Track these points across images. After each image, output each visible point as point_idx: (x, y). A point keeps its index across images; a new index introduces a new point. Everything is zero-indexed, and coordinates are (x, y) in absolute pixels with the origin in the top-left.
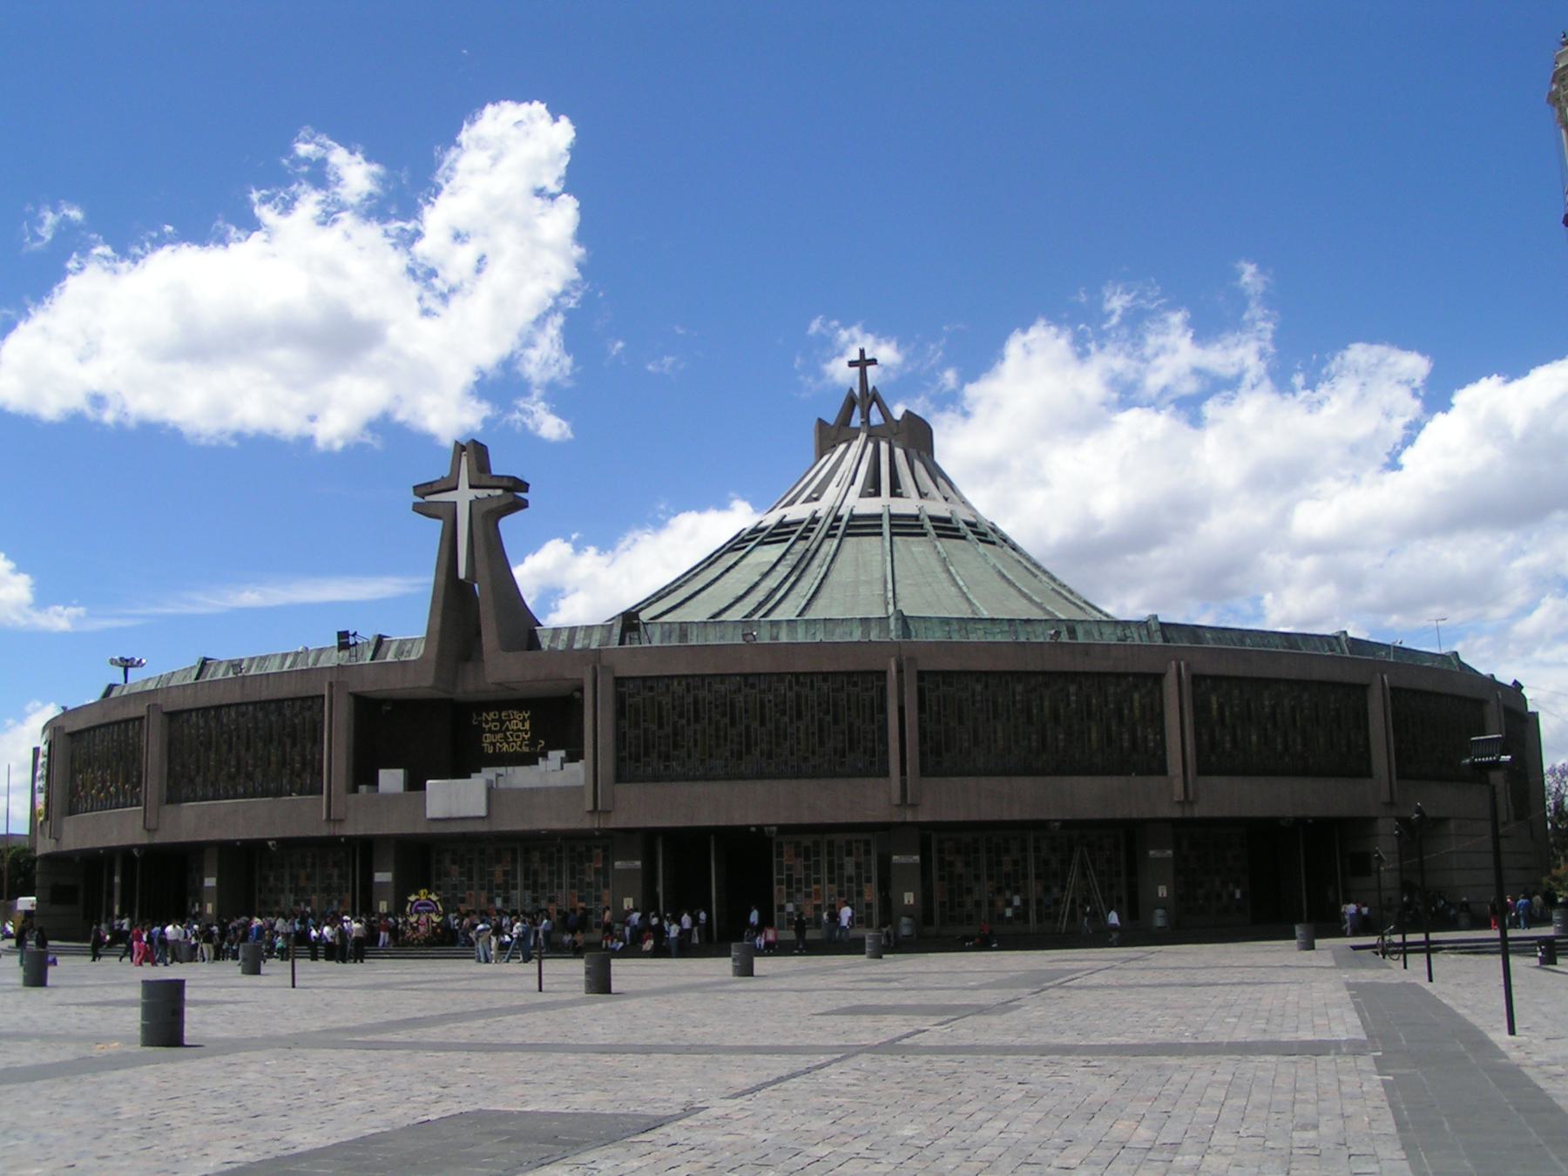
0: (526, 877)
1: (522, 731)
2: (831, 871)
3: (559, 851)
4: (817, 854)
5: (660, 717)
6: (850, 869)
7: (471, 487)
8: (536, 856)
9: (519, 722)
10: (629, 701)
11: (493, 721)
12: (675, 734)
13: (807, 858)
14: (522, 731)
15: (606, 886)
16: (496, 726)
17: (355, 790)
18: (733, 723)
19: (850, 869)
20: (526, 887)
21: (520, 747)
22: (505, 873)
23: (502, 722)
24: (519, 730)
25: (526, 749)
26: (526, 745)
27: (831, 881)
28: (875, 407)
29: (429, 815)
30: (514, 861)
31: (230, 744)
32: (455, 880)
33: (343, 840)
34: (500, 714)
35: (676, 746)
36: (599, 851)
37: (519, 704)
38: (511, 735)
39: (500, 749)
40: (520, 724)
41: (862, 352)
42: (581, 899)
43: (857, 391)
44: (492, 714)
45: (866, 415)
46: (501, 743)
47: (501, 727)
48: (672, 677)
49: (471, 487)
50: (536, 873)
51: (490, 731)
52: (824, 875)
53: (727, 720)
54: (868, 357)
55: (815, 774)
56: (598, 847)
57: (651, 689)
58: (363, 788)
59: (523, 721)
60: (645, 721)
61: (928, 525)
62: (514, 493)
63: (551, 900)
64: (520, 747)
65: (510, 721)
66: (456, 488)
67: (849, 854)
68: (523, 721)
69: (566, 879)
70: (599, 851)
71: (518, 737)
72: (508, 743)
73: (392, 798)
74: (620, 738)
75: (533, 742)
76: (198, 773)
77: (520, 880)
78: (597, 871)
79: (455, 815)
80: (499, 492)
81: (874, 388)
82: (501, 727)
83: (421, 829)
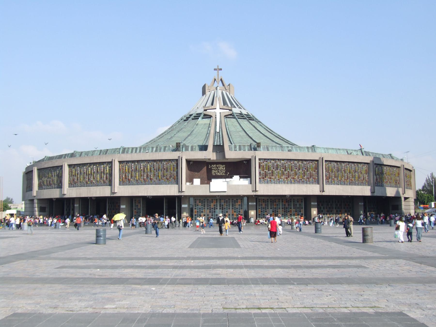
0: (220, 206)
1: (223, 170)
2: (294, 206)
3: (229, 200)
4: (291, 202)
5: (269, 169)
6: (298, 206)
8: (223, 201)
9: (222, 168)
10: (261, 164)
11: (215, 167)
12: (272, 173)
13: (289, 203)
14: (223, 170)
15: (242, 209)
16: (216, 169)
17: (186, 184)
18: (285, 170)
19: (298, 206)
20: (220, 209)
21: (223, 174)
22: (214, 205)
23: (217, 168)
24: (222, 170)
25: (224, 175)
26: (224, 174)
27: (294, 208)
30: (217, 202)
31: (144, 172)
32: (199, 207)
33: (183, 196)
34: (217, 165)
35: (272, 176)
36: (240, 200)
37: (222, 163)
38: (220, 171)
39: (217, 174)
40: (222, 169)
42: (235, 212)
44: (214, 165)
46: (217, 173)
47: (217, 169)
48: (271, 159)
49: (220, 109)
50: (223, 205)
51: (214, 170)
52: (292, 207)
53: (284, 170)
54: (219, 68)
55: (303, 182)
56: (239, 199)
57: (267, 162)
59: (223, 167)
60: (265, 169)
61: (235, 115)
63: (227, 212)
64: (223, 174)
65: (220, 167)
66: (216, 109)
67: (298, 202)
68: (223, 167)
69: (231, 207)
70: (240, 200)
71: (222, 171)
72: (219, 173)
73: (197, 186)
74: (260, 172)
75: (226, 173)
76: (132, 177)
77: (218, 207)
78: (239, 205)
80: (228, 111)
82: (217, 169)
83: (208, 194)
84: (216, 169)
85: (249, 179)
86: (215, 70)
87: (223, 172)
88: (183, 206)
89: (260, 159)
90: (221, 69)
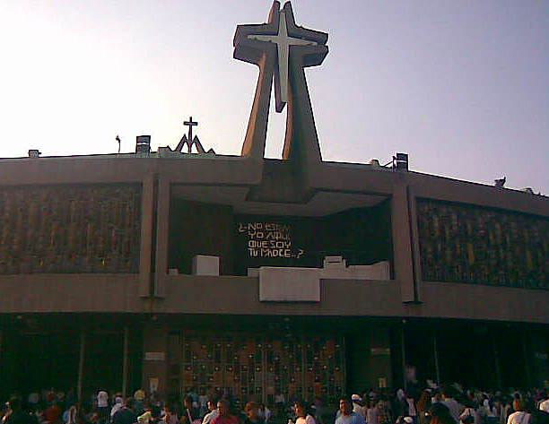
7: (289, 36)
11: (259, 230)
16: (260, 235)
17: (168, 273)
24: (279, 240)
28: (194, 145)
29: (261, 299)
39: (264, 254)
41: (191, 118)
43: (187, 136)
44: (257, 225)
45: (190, 147)
47: (265, 236)
58: (174, 272)
62: (314, 48)
64: (283, 253)
72: (272, 250)
75: (293, 250)
79: (290, 299)
81: (196, 137)
82: (265, 236)
84: (260, 235)
85: (382, 266)
86: (185, 123)
87: (285, 247)
88: (149, 356)
89: (419, 200)
90: (196, 124)
